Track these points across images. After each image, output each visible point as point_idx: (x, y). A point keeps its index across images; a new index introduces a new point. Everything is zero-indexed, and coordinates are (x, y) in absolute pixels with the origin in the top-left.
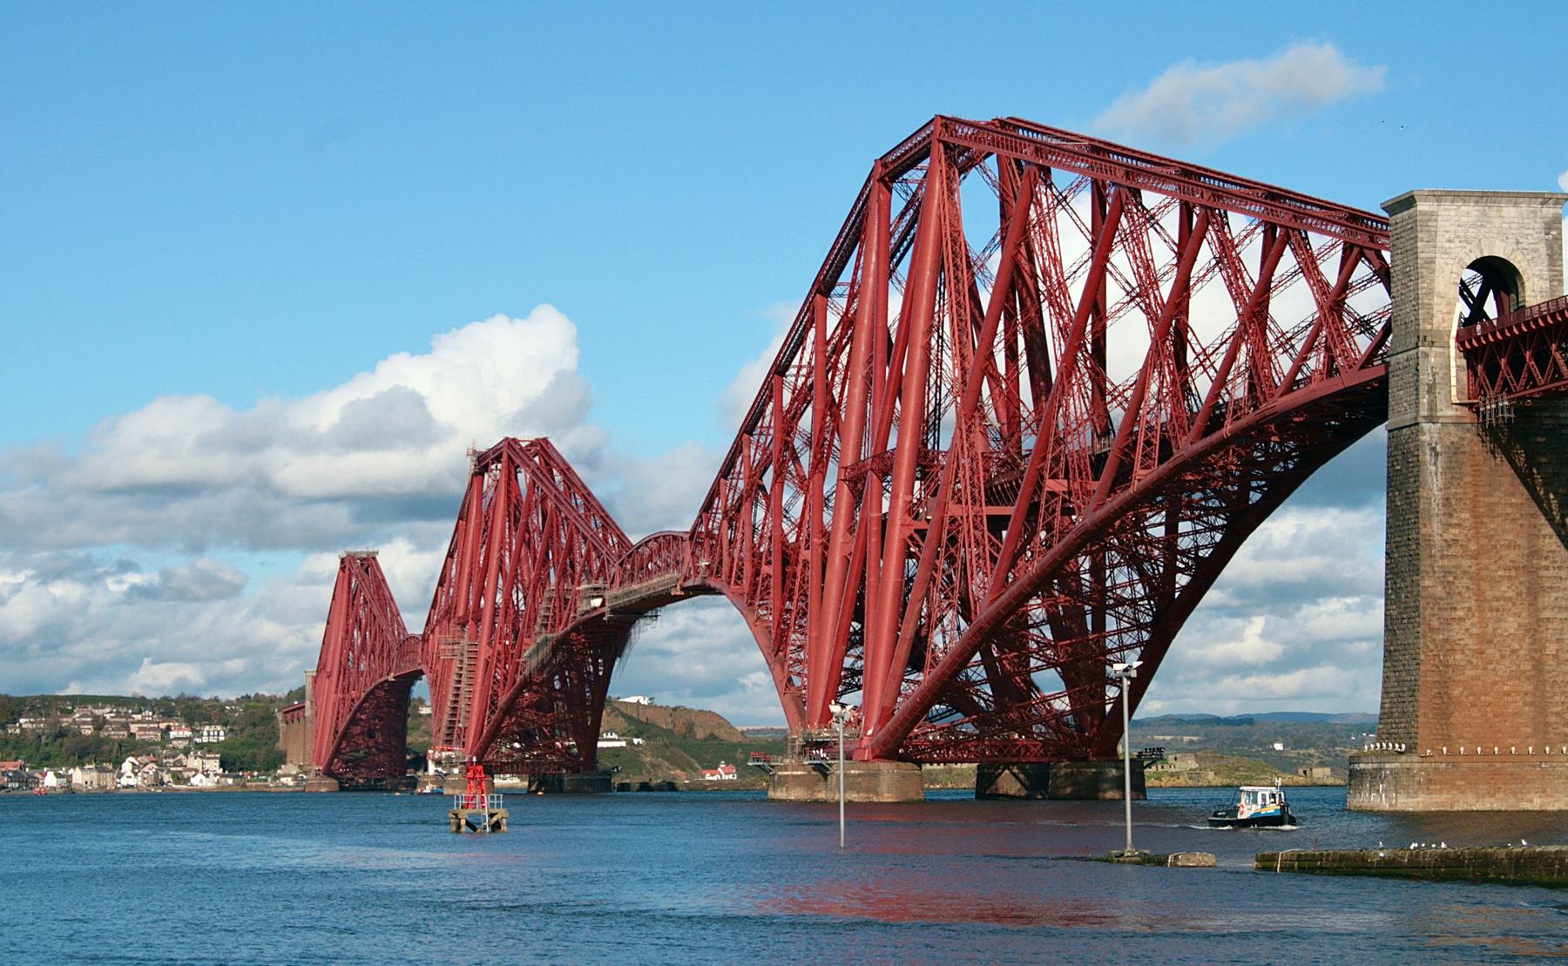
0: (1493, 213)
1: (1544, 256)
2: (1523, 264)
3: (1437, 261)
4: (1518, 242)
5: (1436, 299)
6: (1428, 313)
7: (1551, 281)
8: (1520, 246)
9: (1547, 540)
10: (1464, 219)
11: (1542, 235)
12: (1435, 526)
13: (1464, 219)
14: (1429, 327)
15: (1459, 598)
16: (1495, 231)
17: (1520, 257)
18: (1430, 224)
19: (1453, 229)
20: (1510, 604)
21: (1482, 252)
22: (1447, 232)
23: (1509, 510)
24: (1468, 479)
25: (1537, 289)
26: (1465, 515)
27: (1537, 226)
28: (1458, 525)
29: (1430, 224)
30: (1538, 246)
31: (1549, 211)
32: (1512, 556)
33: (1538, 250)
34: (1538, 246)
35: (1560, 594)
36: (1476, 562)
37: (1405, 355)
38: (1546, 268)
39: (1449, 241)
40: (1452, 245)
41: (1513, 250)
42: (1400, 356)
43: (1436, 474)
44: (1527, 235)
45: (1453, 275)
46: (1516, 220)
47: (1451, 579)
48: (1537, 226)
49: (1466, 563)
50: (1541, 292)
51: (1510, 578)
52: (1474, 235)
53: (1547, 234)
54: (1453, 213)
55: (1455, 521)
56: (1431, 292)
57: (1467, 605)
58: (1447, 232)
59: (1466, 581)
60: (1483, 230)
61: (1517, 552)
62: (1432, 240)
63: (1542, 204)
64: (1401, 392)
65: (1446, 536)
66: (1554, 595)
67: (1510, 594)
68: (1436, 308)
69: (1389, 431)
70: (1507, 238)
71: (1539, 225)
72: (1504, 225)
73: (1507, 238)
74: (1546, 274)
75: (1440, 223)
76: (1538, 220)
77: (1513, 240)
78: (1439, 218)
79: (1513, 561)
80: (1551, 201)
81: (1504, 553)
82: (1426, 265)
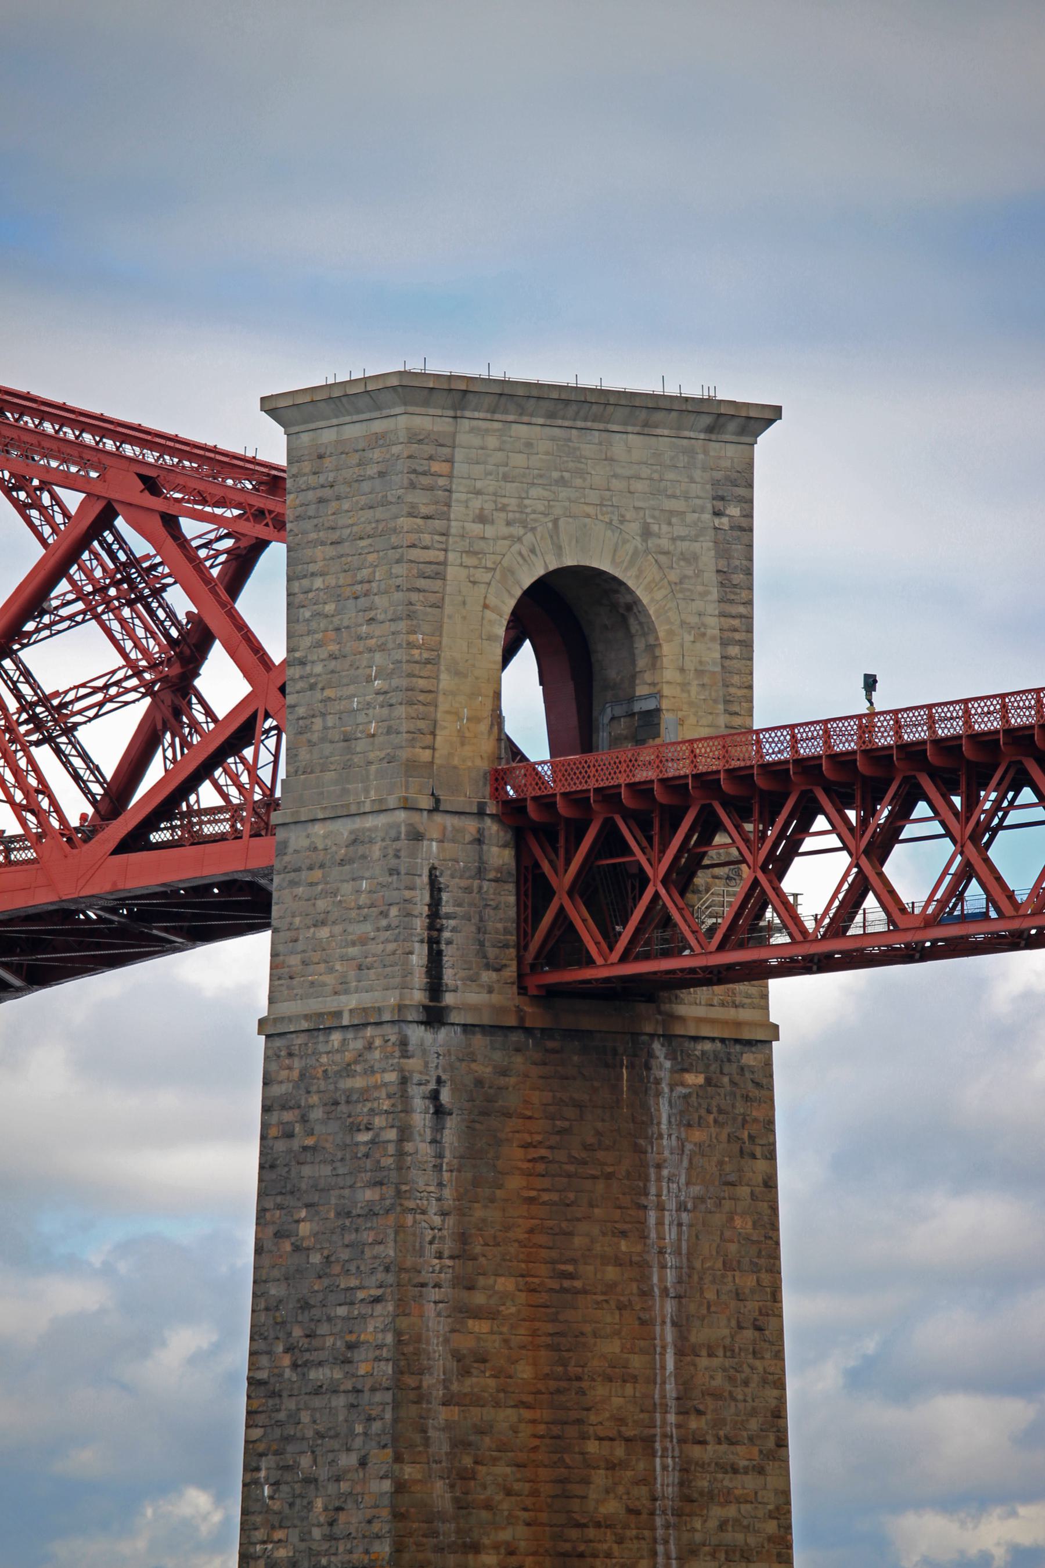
0: (589, 446)
1: (710, 577)
2: (659, 595)
3: (451, 572)
4: (646, 533)
5: (446, 681)
7: (724, 643)
8: (650, 543)
9: (703, 1362)
10: (519, 460)
11: (707, 516)
12: (430, 1310)
14: (426, 755)
15: (485, 1515)
16: (593, 496)
17: (652, 573)
18: (436, 467)
19: (489, 485)
20: (609, 1536)
22: (478, 493)
23: (611, 1273)
24: (515, 1182)
25: (690, 664)
26: (505, 1284)
27: (695, 489)
28: (492, 1315)
29: (436, 467)
30: (696, 546)
31: (728, 452)
32: (617, 1401)
33: (696, 557)
35: (731, 1511)
36: (527, 1414)
37: (344, 828)
38: (713, 608)
39: (482, 519)
40: (490, 531)
41: (636, 553)
42: (319, 829)
43: (438, 1168)
44: (672, 513)
45: (488, 614)
46: (645, 472)
47: (467, 1461)
48: (695, 489)
49: (505, 1417)
50: (700, 673)
51: (611, 1466)
52: (540, 506)
53: (717, 514)
54: (492, 442)
55: (479, 1299)
57: (505, 1535)
58: (478, 493)
59: (503, 1470)
60: (564, 493)
61: (629, 1389)
63: (710, 429)
64: (324, 933)
65: (465, 1343)
66: (717, 1512)
67: (612, 1507)
68: (444, 704)
69: (268, 1036)
70: (623, 520)
71: (700, 490)
72: (616, 484)
73: (623, 520)
74: (713, 623)
75: (460, 468)
76: (698, 474)
77: (634, 528)
78: (459, 455)
79: (621, 1421)
80: (732, 426)
81: (600, 1390)
82: (422, 583)
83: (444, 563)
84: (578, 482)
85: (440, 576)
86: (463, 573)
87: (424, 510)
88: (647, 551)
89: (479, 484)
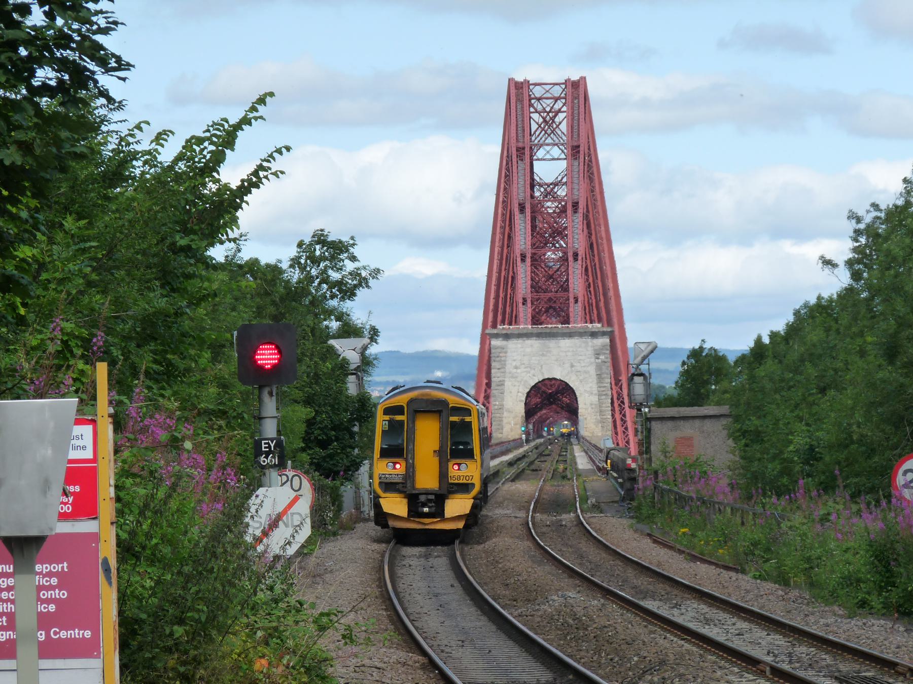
0: (552, 343)
1: (594, 377)
4: (572, 366)
5: (505, 414)
6: (499, 425)
11: (593, 360)
13: (528, 350)
17: (574, 377)
21: (543, 374)
22: (514, 360)
30: (589, 369)
34: (589, 369)
39: (516, 368)
40: (519, 371)
45: (520, 394)
54: (519, 346)
56: (501, 408)
58: (514, 360)
60: (544, 358)
62: (503, 366)
68: (505, 421)
71: (590, 351)
74: (595, 389)
78: (509, 351)
83: (504, 381)
84: (549, 354)
85: (503, 385)
86: (510, 383)
87: (498, 367)
88: (572, 372)
89: (515, 358)
